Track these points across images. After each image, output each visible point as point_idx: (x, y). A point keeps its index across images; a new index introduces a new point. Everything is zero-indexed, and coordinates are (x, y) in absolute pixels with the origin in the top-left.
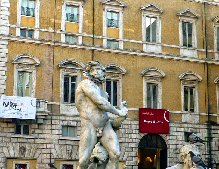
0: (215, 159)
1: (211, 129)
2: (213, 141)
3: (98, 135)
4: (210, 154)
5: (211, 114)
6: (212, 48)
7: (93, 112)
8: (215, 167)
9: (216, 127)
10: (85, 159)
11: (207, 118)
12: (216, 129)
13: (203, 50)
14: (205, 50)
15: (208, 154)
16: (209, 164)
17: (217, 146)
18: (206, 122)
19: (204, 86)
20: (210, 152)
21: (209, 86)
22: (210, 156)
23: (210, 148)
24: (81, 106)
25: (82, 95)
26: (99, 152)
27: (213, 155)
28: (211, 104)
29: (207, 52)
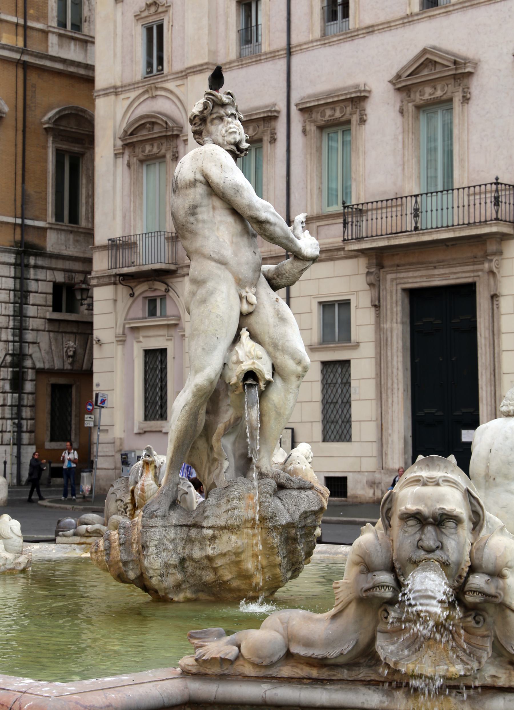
0: (33, 356)
1: (27, 266)
2: (31, 303)
3: (246, 308)
4: (22, 341)
5: (29, 222)
6: (43, 17)
7: (234, 240)
8: (31, 380)
9: (40, 262)
11: (18, 231)
12: (42, 267)
13: (14, 19)
14: (21, 21)
15: (14, 342)
16: (16, 371)
17: (42, 316)
18: (13, 244)
19: (11, 133)
20: (21, 336)
21: (28, 135)
22: (21, 347)
23: (21, 322)
24: (197, 220)
25: (201, 189)
26: (250, 355)
27: (29, 343)
28: (31, 190)
29: (25, 27)
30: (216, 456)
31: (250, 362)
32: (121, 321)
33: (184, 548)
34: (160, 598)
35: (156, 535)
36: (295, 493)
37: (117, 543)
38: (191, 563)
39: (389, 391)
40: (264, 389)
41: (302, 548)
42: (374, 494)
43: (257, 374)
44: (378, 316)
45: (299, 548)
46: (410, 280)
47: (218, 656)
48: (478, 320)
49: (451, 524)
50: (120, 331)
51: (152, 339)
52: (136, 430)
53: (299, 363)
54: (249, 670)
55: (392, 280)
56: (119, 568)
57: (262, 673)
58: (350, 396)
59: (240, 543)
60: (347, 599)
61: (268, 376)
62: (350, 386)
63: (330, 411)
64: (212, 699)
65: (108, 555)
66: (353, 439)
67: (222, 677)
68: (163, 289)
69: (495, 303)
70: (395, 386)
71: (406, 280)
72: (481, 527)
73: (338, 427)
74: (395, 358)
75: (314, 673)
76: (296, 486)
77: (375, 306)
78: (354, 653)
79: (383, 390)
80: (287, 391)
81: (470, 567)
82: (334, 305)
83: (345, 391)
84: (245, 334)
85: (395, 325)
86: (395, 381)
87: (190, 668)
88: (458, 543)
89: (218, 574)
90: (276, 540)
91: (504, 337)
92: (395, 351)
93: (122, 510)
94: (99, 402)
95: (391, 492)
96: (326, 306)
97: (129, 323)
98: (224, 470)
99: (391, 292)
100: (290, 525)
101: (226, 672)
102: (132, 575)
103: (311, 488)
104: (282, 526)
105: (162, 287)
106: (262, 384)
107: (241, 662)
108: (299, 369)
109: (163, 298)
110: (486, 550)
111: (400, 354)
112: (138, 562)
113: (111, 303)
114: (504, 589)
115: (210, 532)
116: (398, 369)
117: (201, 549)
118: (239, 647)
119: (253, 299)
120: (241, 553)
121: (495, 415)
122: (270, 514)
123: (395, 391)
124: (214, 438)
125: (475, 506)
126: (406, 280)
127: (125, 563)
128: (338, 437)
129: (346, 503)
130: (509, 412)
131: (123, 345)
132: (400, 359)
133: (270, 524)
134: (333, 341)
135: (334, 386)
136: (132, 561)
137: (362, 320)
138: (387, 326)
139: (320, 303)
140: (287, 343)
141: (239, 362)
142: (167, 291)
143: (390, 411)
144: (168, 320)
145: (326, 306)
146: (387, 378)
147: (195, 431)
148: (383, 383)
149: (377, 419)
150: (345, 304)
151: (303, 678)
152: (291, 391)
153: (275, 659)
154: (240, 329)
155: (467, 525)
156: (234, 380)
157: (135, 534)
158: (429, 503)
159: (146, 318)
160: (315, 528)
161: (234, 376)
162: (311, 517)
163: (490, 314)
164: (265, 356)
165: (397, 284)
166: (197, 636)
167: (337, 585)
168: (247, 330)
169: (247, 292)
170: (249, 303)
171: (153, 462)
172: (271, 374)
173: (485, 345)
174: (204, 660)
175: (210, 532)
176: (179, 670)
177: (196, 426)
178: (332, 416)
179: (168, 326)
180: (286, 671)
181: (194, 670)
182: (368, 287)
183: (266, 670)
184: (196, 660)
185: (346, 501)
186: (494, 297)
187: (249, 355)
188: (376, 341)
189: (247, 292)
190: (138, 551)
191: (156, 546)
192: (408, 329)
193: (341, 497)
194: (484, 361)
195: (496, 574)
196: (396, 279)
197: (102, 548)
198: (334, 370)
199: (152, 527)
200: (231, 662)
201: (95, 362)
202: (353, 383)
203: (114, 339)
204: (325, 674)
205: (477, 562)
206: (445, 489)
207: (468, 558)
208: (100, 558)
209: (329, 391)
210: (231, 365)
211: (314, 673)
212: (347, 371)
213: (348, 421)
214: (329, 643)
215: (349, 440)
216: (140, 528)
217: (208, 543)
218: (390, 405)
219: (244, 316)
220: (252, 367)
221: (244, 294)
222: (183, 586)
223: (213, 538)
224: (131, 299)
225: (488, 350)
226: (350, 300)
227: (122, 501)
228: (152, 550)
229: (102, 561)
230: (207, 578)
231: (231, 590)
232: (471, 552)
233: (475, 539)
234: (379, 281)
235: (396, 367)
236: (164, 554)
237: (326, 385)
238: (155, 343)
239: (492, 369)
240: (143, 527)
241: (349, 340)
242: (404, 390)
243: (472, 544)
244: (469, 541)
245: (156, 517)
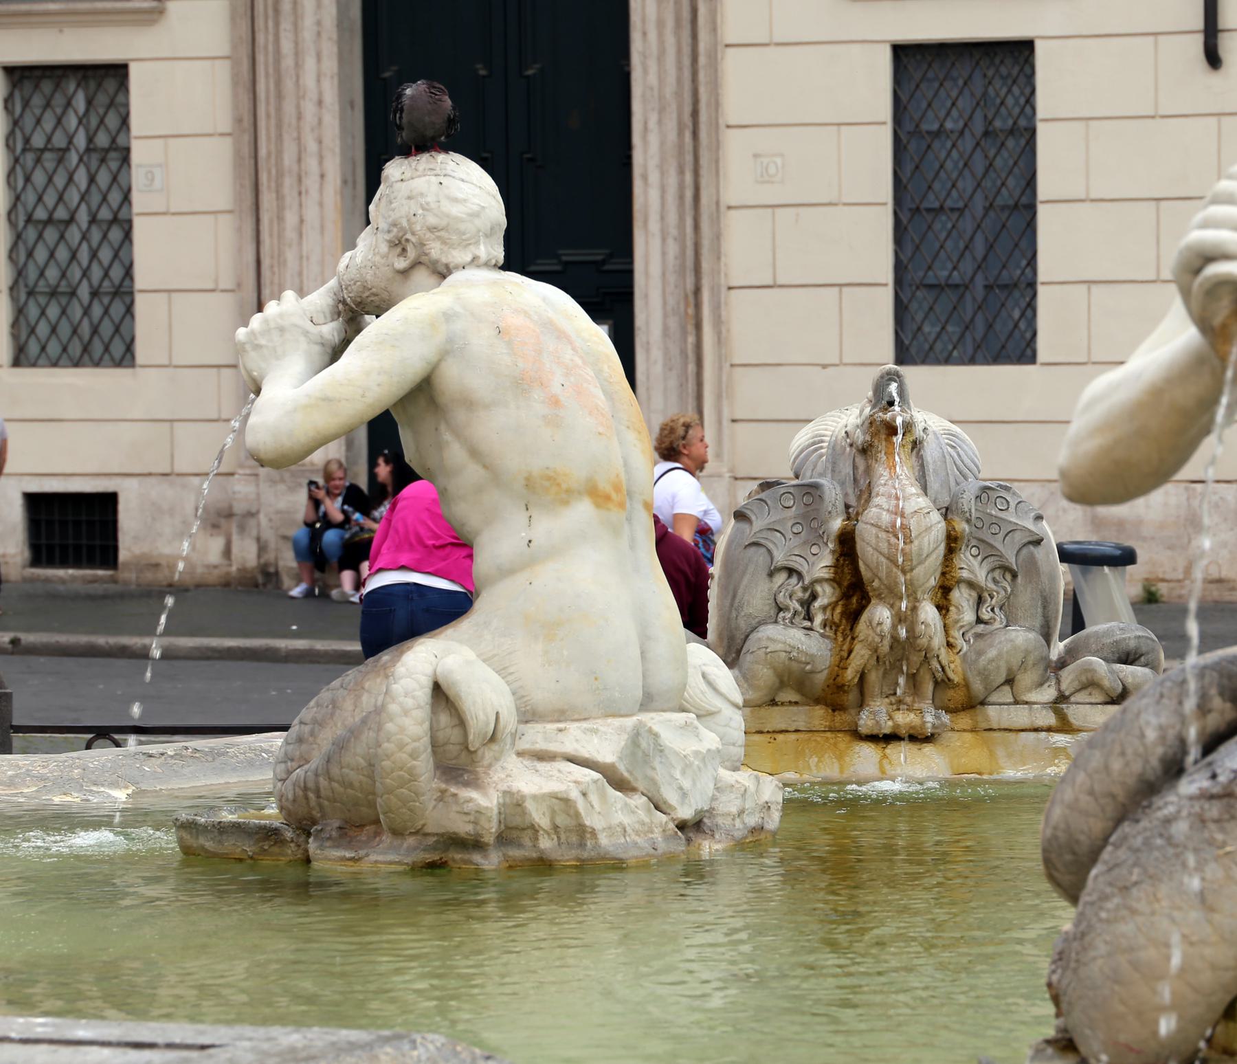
39: (288, 182)
42: (227, 552)
58: (126, 198)
70: (311, 164)
73: (76, 311)
74: (310, 63)
79: (263, 177)
83: (103, 178)
86: (312, 146)
92: (308, 35)
111: (330, 50)
116: (320, 103)
123: (312, 182)
128: (76, 349)
129: (112, 588)
132: (330, 64)
135: (60, 161)
143: (291, 256)
146: (280, 137)
148: (263, 152)
149: (239, 285)
173: (660, 24)
178: (52, 274)
185: (114, 580)
193: (91, 563)
194: (653, 79)
198: (59, 100)
209: (39, 178)
212: (111, 104)
213: (122, 292)
215: (126, 358)
218: (290, 234)
225: (670, 40)
235: (312, 94)
239: (688, 109)
242: (345, 182)
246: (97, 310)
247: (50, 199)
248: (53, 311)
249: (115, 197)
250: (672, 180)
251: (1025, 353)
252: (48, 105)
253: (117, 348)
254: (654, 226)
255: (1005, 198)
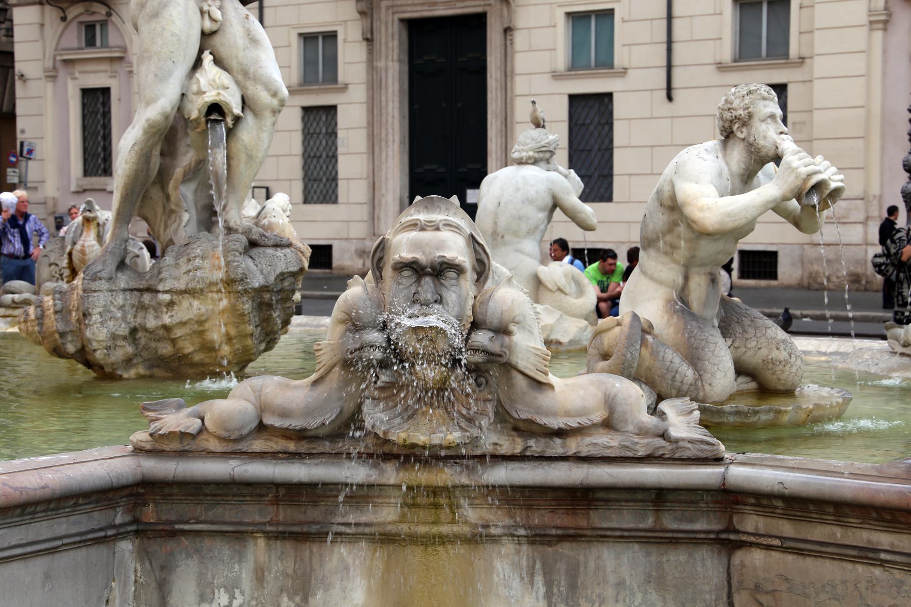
3: (208, 25)
10: (168, 109)
26: (213, 84)
30: (173, 207)
31: (214, 93)
32: (50, 51)
33: (135, 316)
34: (106, 375)
35: (100, 300)
36: (270, 251)
37: (51, 311)
38: (144, 334)
39: (383, 143)
40: (231, 126)
41: (278, 316)
42: (364, 264)
43: (224, 107)
44: (371, 52)
45: (275, 315)
46: (409, 9)
47: (177, 430)
48: (489, 58)
49: (452, 274)
50: (49, 64)
51: (92, 76)
52: (73, 188)
53: (275, 95)
54: (214, 445)
55: (388, 8)
56: (55, 340)
57: (230, 447)
58: (336, 149)
59: (203, 310)
60: (330, 363)
61: (237, 110)
62: (336, 136)
63: (312, 167)
64: (171, 477)
65: (41, 324)
66: (340, 199)
67: (182, 454)
68: (104, 12)
69: (509, 38)
70: (390, 137)
71: (404, 9)
72: (486, 278)
73: (321, 186)
75: (291, 446)
76: (271, 243)
77: (367, 40)
78: (338, 422)
80: (260, 129)
81: (472, 323)
82: (317, 38)
83: (330, 142)
84: (207, 58)
85: (390, 64)
86: (390, 131)
87: (143, 444)
88: (460, 296)
89: (178, 346)
90: (247, 306)
91: (518, 79)
92: (390, 95)
93: (57, 276)
94: (25, 152)
95: (383, 239)
96: (308, 39)
97: (61, 55)
98: (183, 224)
99: (386, 23)
100: (264, 289)
101: (187, 448)
102: (71, 348)
103: (289, 245)
104: (254, 289)
105: (103, 10)
106: (229, 120)
107: (205, 436)
108: (275, 102)
109: (104, 24)
110: (491, 304)
111: (397, 99)
112: (79, 333)
113: (36, 28)
114: (509, 347)
115: (167, 297)
116: (393, 117)
117: (157, 317)
118: (203, 419)
119: (217, 15)
120: (205, 321)
121: (506, 162)
122: (240, 276)
123: (390, 143)
124: (171, 185)
125: (480, 254)
126: (404, 9)
127: (62, 335)
128: (321, 198)
129: (329, 275)
130: (522, 159)
131: (54, 81)
132: (397, 104)
133: (240, 288)
134: (316, 82)
135: (318, 137)
136: (71, 331)
137: (351, 57)
138: (381, 64)
139: (300, 35)
140: (259, 70)
141: (200, 93)
142: (109, 15)
143: (384, 167)
144: (111, 52)
145: (308, 39)
146: (381, 129)
147: (147, 176)
149: (368, 177)
150: (331, 37)
151: (279, 452)
152: (265, 129)
153: (245, 432)
154: (201, 51)
155: (470, 275)
156: (194, 115)
157: (74, 300)
158: (428, 250)
159: (82, 49)
160: (293, 292)
161: (195, 110)
162: (289, 279)
163: (503, 51)
164: (233, 87)
165: (393, 14)
166: (152, 408)
167: (319, 347)
168: (211, 53)
169: (210, 6)
170: (212, 19)
171: (95, 218)
172: (240, 107)
173: (496, 89)
174: (161, 435)
175: (167, 297)
176: (130, 447)
177: (148, 170)
178: (315, 174)
179: (112, 59)
180: (258, 445)
181: (148, 447)
182: (358, 16)
183: (234, 444)
184: (151, 435)
185: (331, 273)
186: (508, 31)
187: (213, 84)
188: (367, 83)
189: (210, 6)
190: (78, 320)
191: (100, 313)
192: (406, 68)
194: (494, 107)
195: (502, 330)
196: (392, 6)
197: (32, 317)
198: (318, 117)
199: (95, 291)
200: (193, 437)
201: (19, 103)
202: (341, 134)
203: (41, 74)
204: (303, 447)
205: (480, 317)
206: (446, 235)
207: (470, 313)
208: (30, 329)
209: (312, 143)
210: (191, 96)
211: (291, 446)
213: (334, 179)
214: (308, 412)
215: (335, 201)
216: (81, 292)
217: (165, 310)
218: (384, 160)
219: (206, 36)
220: (217, 98)
221: (206, 8)
222: (135, 361)
223: (171, 304)
224: (63, 25)
225: (499, 94)
226: (336, 32)
227: (57, 265)
228: (96, 318)
229: (33, 332)
230: (164, 351)
231: (193, 365)
232: (474, 306)
233: (479, 292)
234: (372, 8)
235: (391, 114)
236: (111, 323)
237: (308, 135)
238: (96, 81)
240: (84, 291)
241: (335, 80)
242: (401, 143)
243: (475, 297)
244: (472, 294)
245: (100, 279)
246: (328, 184)
247: (315, 149)
248: (315, 186)
249: (333, 148)
250: (499, 141)
251: (609, 199)
252: (315, 119)
253: (333, 198)
254: (494, 156)
255: (603, 147)
